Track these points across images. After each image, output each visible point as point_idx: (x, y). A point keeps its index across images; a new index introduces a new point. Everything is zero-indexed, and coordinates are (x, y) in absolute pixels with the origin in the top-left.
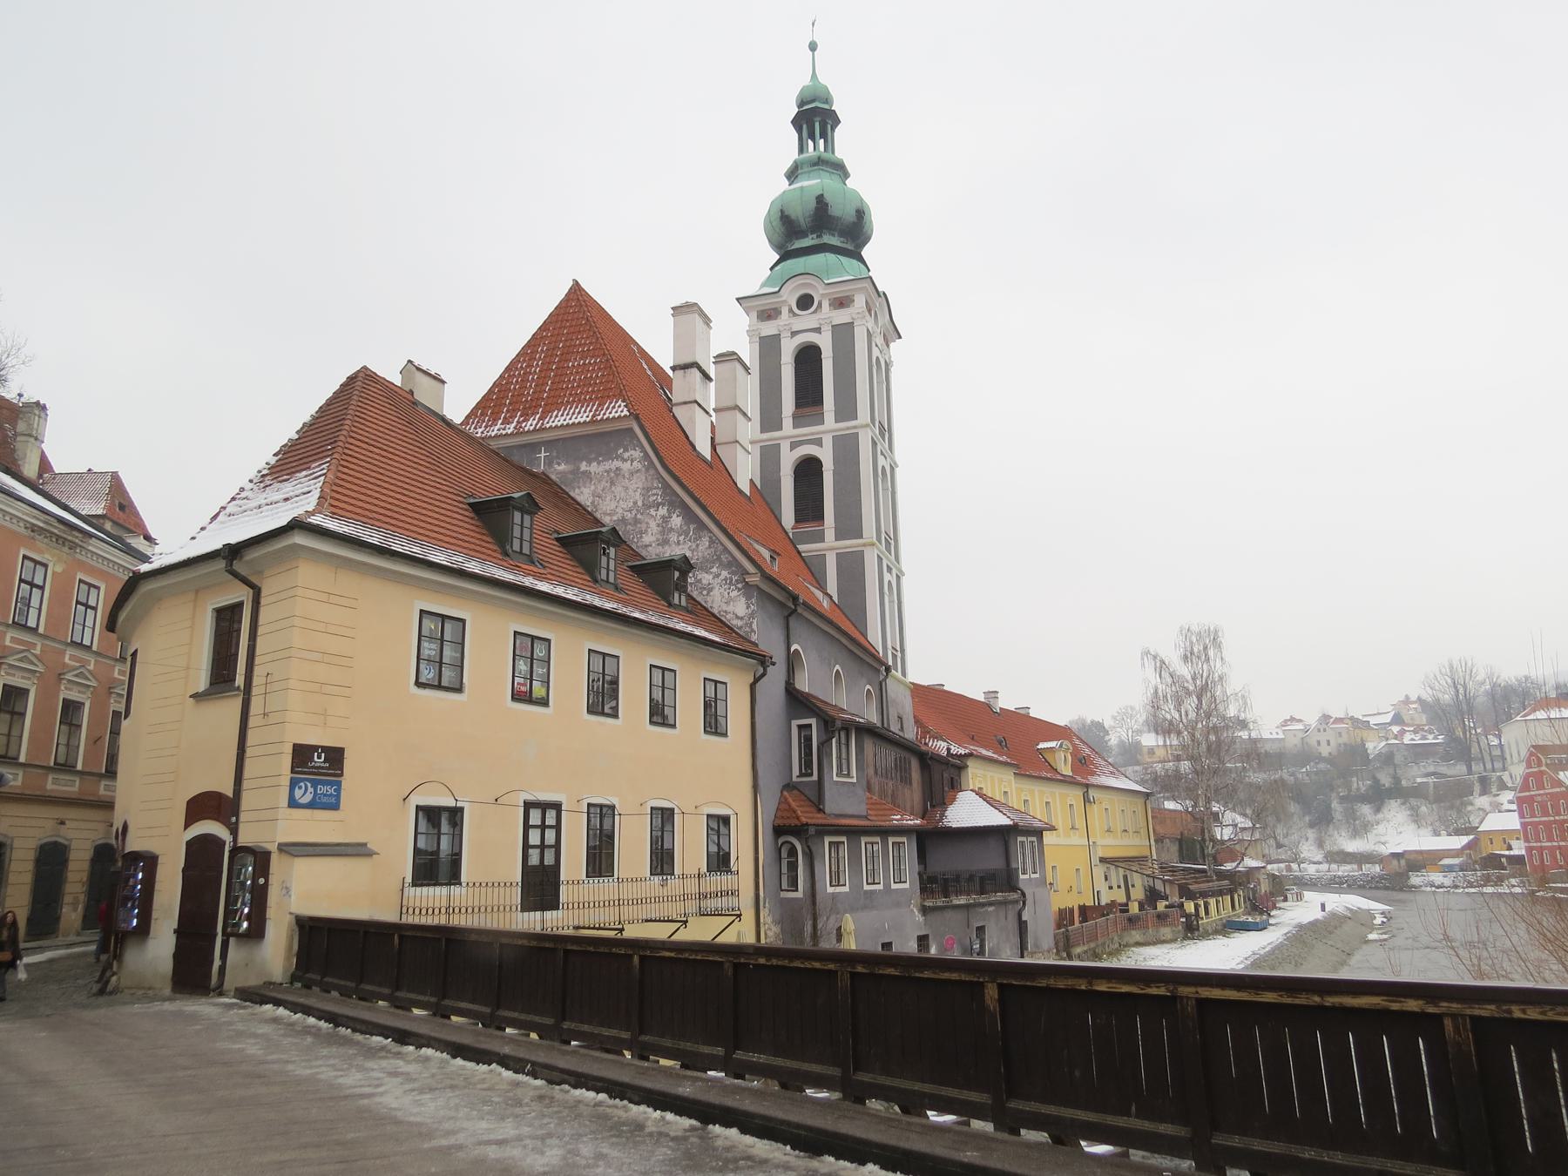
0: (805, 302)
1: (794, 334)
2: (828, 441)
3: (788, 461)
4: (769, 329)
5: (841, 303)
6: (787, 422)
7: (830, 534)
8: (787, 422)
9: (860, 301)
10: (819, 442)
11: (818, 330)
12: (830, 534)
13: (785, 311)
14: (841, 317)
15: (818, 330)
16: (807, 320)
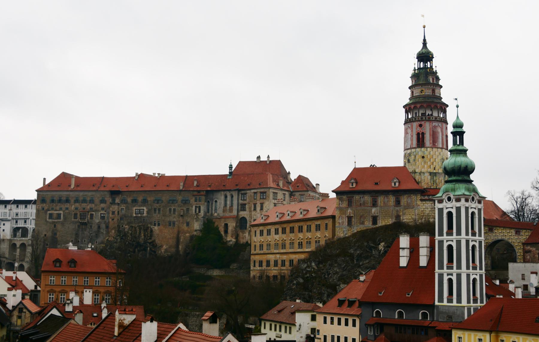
0: (449, 199)
1: (447, 208)
2: (455, 241)
3: (446, 245)
4: (440, 206)
5: (458, 200)
6: (445, 234)
7: (455, 267)
8: (445, 234)
9: (463, 200)
10: (452, 241)
11: (452, 208)
12: (455, 267)
13: (444, 201)
14: (458, 204)
15: (452, 208)
16: (449, 204)
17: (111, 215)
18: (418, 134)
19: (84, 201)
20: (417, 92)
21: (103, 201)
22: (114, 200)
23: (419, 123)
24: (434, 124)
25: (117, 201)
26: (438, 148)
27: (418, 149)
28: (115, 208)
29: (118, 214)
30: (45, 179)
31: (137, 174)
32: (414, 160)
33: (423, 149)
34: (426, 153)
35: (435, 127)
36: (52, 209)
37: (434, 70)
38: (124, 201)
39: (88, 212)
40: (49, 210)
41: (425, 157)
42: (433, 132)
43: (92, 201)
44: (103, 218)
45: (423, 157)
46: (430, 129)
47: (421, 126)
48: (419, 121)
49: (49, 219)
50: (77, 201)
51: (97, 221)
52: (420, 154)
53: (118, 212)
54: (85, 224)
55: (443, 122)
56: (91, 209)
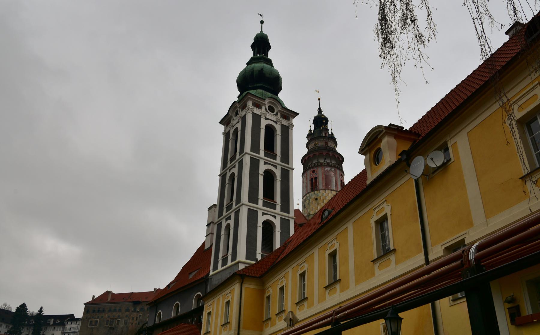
17: (131, 321)
18: (312, 179)
19: (115, 311)
20: (311, 146)
21: (127, 310)
22: (135, 309)
23: (313, 170)
24: (326, 169)
25: (138, 309)
26: (331, 190)
27: (312, 193)
28: (135, 314)
29: (137, 319)
30: (94, 296)
31: (155, 289)
32: (309, 204)
33: (316, 192)
34: (319, 195)
35: (327, 171)
36: (93, 318)
37: (330, 133)
38: (142, 310)
39: (116, 319)
40: (90, 319)
41: (319, 198)
42: (326, 176)
43: (120, 311)
44: (126, 323)
45: (316, 199)
46: (322, 173)
47: (313, 172)
48: (312, 167)
49: (90, 325)
50: (110, 311)
51: (122, 326)
52: (314, 196)
53: (137, 318)
54: (112, 328)
55: (337, 168)
56: (119, 316)
